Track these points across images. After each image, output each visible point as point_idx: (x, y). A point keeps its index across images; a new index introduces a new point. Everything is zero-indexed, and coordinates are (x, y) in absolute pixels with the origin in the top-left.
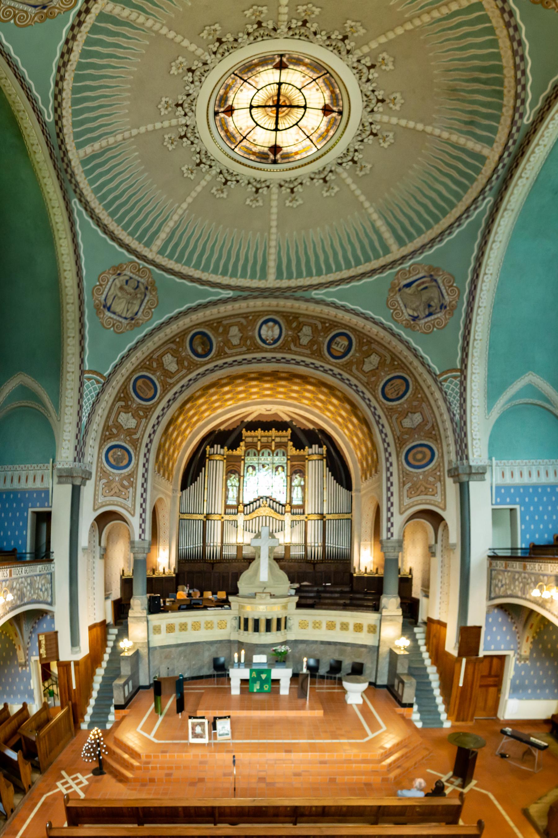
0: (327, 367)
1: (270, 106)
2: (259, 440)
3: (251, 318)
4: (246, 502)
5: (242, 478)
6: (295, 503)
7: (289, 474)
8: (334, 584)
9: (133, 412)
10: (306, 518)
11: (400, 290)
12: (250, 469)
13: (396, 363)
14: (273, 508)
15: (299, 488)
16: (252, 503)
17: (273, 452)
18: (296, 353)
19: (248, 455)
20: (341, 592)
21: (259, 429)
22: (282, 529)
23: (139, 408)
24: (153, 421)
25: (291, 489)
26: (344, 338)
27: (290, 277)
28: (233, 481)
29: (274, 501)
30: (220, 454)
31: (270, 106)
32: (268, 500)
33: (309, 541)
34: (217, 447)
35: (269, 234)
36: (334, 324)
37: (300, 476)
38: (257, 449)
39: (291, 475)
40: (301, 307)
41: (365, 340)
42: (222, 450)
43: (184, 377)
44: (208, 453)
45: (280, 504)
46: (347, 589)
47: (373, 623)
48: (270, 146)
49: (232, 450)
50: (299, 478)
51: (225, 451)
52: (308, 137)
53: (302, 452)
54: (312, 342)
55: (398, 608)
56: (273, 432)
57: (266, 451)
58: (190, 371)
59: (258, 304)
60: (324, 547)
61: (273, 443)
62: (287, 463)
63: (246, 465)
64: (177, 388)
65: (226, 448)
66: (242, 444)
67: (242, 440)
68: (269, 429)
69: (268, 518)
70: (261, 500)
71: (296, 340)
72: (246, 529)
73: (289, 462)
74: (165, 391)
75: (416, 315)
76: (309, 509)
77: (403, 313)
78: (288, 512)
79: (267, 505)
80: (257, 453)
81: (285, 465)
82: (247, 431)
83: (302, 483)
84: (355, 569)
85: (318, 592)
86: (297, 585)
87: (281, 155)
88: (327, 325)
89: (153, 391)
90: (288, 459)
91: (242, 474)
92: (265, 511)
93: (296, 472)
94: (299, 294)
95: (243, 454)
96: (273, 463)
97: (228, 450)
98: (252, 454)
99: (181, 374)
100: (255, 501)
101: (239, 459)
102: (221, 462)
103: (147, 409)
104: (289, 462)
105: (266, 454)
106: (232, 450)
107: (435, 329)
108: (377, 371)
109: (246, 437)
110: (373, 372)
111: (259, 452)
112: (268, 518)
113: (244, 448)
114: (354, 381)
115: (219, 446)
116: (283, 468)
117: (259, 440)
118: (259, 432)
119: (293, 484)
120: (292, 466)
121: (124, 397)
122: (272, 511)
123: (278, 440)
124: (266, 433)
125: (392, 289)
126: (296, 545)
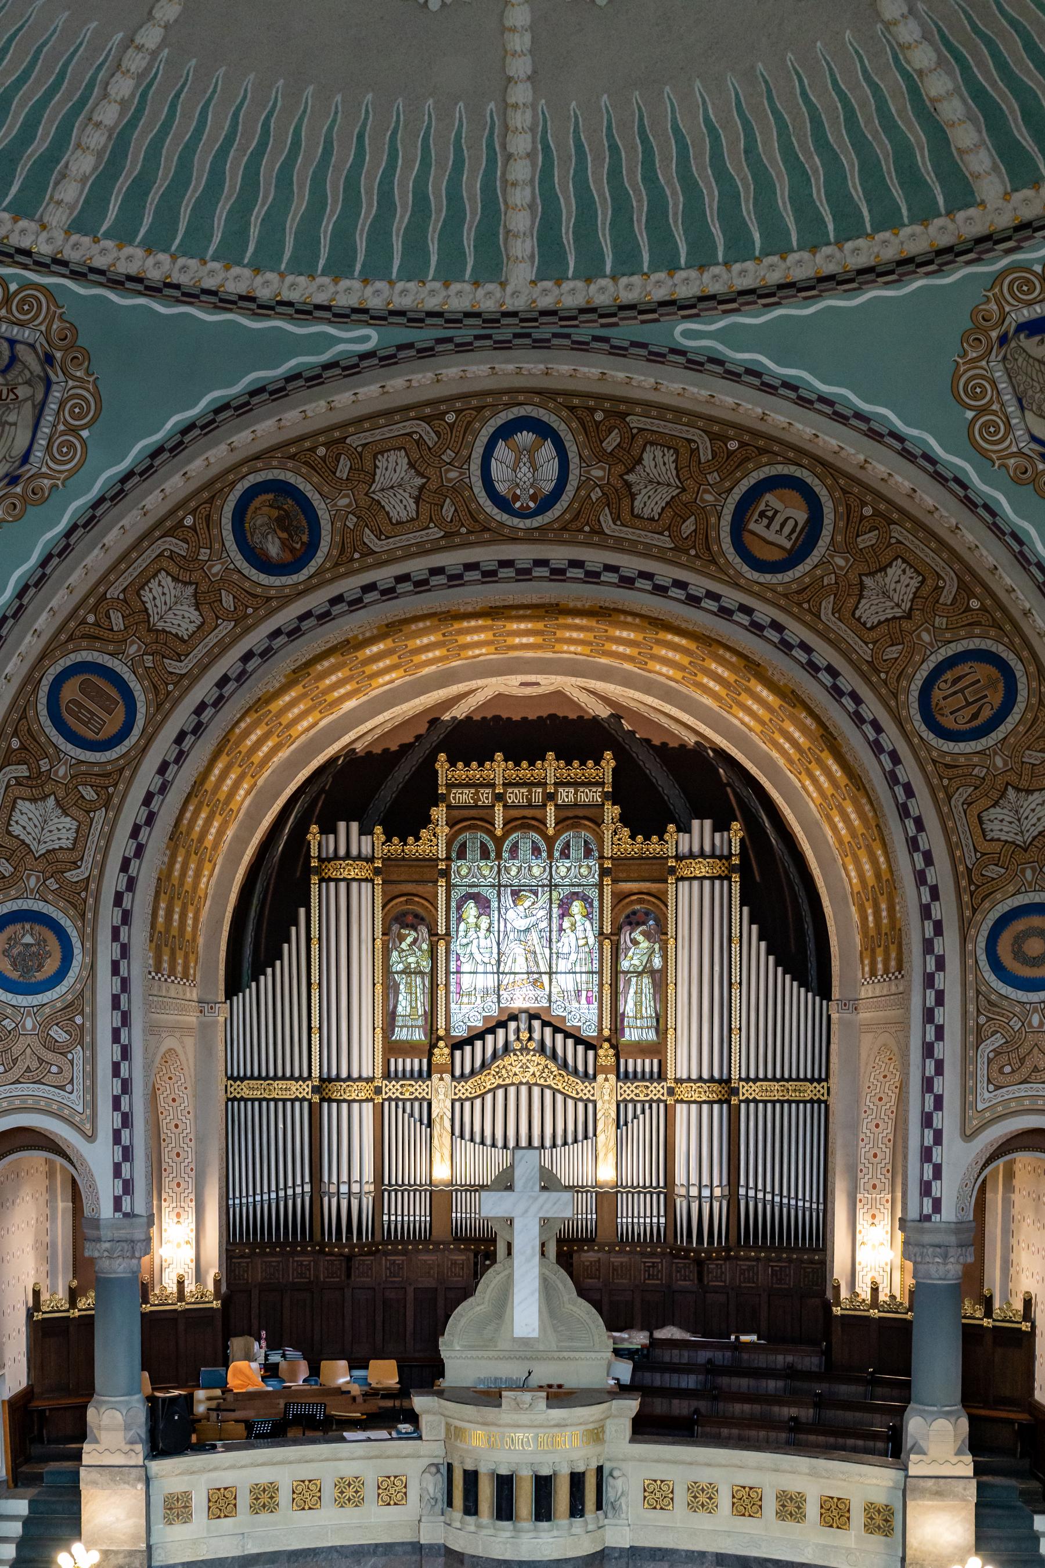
0: (732, 597)
2: (499, 797)
3: (451, 418)
4: (459, 1032)
5: (442, 943)
6: (631, 1035)
7: (607, 929)
8: (774, 1339)
9: (61, 793)
10: (671, 1092)
12: (471, 910)
13: (974, 604)
14: (554, 1056)
15: (646, 980)
16: (481, 1036)
17: (550, 841)
18: (619, 546)
19: (462, 855)
20: (791, 1373)
21: (499, 756)
22: (588, 1133)
23: (81, 774)
24: (132, 811)
25: (613, 982)
27: (590, 273)
28: (410, 953)
29: (556, 1030)
30: (359, 857)
32: (536, 1024)
33: (680, 1177)
34: (348, 831)
35: (505, 107)
36: (759, 444)
37: (647, 935)
38: (491, 833)
39: (617, 931)
40: (639, 380)
42: (366, 840)
43: (223, 647)
44: (314, 852)
45: (578, 1041)
46: (811, 1362)
47: (880, 1498)
49: (404, 840)
50: (645, 944)
51: (373, 843)
53: (654, 846)
54: (678, 509)
55: (959, 1452)
56: (550, 768)
57: (525, 840)
58: (243, 624)
59: (478, 371)
60: (732, 1198)
61: (551, 809)
62: (600, 886)
63: (456, 895)
64: (203, 690)
65: (378, 829)
66: (439, 813)
67: (436, 800)
68: (535, 756)
69: (536, 1091)
70: (512, 1025)
71: (620, 497)
72: (458, 1133)
73: (607, 881)
74: (163, 704)
76: (683, 1059)
78: (605, 1070)
79: (532, 1045)
80: (491, 846)
81: (593, 893)
82: (453, 764)
83: (657, 963)
84: (837, 1289)
85: (711, 1369)
86: (638, 1339)
89: (120, 712)
90: (604, 872)
91: (441, 930)
92: (525, 1067)
93: (633, 921)
94: (627, 330)
95: (442, 855)
96: (552, 886)
97: (389, 839)
98: (473, 852)
99: (212, 639)
100: (492, 1031)
101: (432, 871)
102: (366, 887)
103: (108, 775)
104: (607, 881)
105: (525, 847)
106: (404, 840)
108: (906, 625)
109: (450, 786)
110: (894, 630)
111: (499, 842)
112: (536, 1091)
113: (443, 831)
114: (825, 654)
115: (355, 826)
117: (499, 797)
118: (499, 768)
119: (625, 965)
120: (619, 898)
121: (23, 747)
122: (552, 1066)
123: (566, 796)
124: (525, 771)
126: (635, 1190)
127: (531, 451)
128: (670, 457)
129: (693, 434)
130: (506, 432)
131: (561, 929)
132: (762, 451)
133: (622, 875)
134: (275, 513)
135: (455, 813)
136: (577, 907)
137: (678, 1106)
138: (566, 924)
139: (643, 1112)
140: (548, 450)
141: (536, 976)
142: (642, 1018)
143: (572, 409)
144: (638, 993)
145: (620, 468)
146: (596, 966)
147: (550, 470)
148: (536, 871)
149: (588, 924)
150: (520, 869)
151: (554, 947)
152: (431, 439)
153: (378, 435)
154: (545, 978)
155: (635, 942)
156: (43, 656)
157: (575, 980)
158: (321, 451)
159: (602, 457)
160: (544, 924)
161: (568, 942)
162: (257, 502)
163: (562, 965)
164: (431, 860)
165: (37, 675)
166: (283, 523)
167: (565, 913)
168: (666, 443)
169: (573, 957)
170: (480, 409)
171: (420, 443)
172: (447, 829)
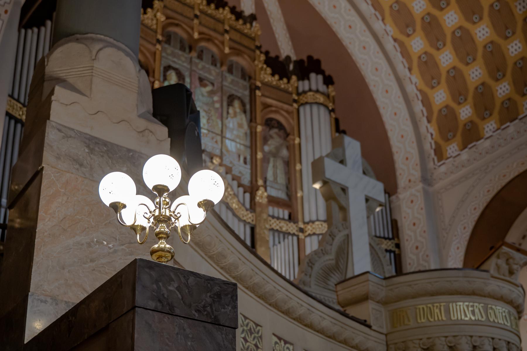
2: (196, 16)
81: (247, 100)
83: (285, 152)
116: (243, 104)
131: (228, 113)
133: (267, 94)
135: (169, 13)
136: (237, 104)
137: (308, 240)
138: (231, 111)
139: (279, 243)
141: (214, 135)
142: (277, 183)
144: (275, 167)
146: (248, 143)
148: (213, 73)
149: (243, 116)
150: (204, 68)
151: (224, 119)
154: (219, 138)
155: (271, 137)
157: (236, 147)
160: (217, 105)
161: (231, 123)
163: (228, 135)
164: (152, 30)
167: (230, 104)
169: (235, 132)
172: (163, 19)
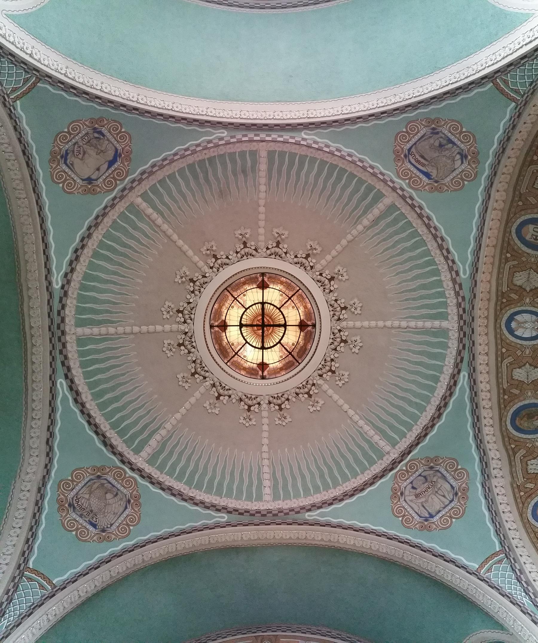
1: (263, 333)
11: (436, 182)
26: (524, 231)
31: (263, 333)
41: (520, 203)
48: (299, 331)
52: (235, 299)
75: (458, 157)
77: (463, 171)
87: (308, 320)
88: (509, 255)
107: (464, 130)
125: (440, 190)
127: (519, 323)
128: (517, 274)
129: (507, 267)
130: (511, 332)
132: (509, 244)
134: (525, 419)
140: (518, 317)
143: (501, 309)
145: (524, 293)
147: (527, 317)
152: (510, 359)
153: (505, 377)
156: (521, 515)
158: (506, 397)
159: (521, 299)
162: (517, 423)
165: (526, 521)
166: (530, 417)
168: (512, 275)
170: (502, 340)
171: (511, 364)
